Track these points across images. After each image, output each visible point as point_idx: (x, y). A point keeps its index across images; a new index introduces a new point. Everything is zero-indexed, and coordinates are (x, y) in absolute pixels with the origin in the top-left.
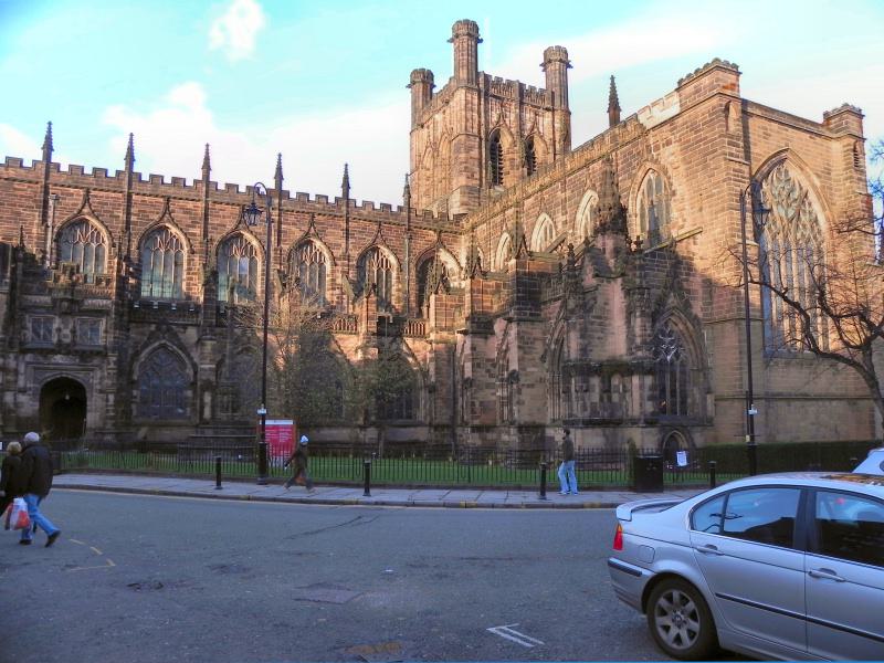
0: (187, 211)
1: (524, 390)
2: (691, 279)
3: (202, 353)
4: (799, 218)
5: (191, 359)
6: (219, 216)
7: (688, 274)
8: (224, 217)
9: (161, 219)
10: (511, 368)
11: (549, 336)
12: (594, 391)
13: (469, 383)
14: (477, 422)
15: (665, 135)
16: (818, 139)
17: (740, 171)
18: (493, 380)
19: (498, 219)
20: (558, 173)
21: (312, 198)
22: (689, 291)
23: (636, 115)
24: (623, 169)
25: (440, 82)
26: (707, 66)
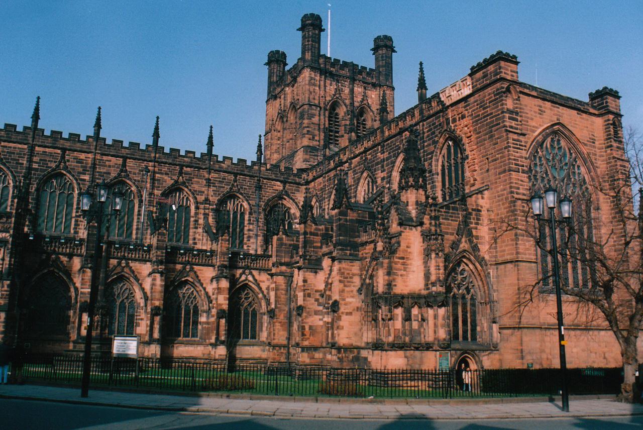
0: (80, 161)
1: (344, 317)
2: (479, 227)
4: (569, 179)
6: (106, 166)
7: (477, 224)
8: (110, 166)
9: (57, 166)
10: (334, 299)
11: (365, 273)
12: (397, 320)
13: (300, 309)
14: (306, 343)
15: (461, 110)
16: (584, 115)
17: (518, 140)
18: (321, 308)
19: (332, 174)
20: (379, 138)
21: (182, 153)
22: (477, 237)
23: (438, 93)
24: (428, 136)
25: (291, 61)
26: (492, 56)
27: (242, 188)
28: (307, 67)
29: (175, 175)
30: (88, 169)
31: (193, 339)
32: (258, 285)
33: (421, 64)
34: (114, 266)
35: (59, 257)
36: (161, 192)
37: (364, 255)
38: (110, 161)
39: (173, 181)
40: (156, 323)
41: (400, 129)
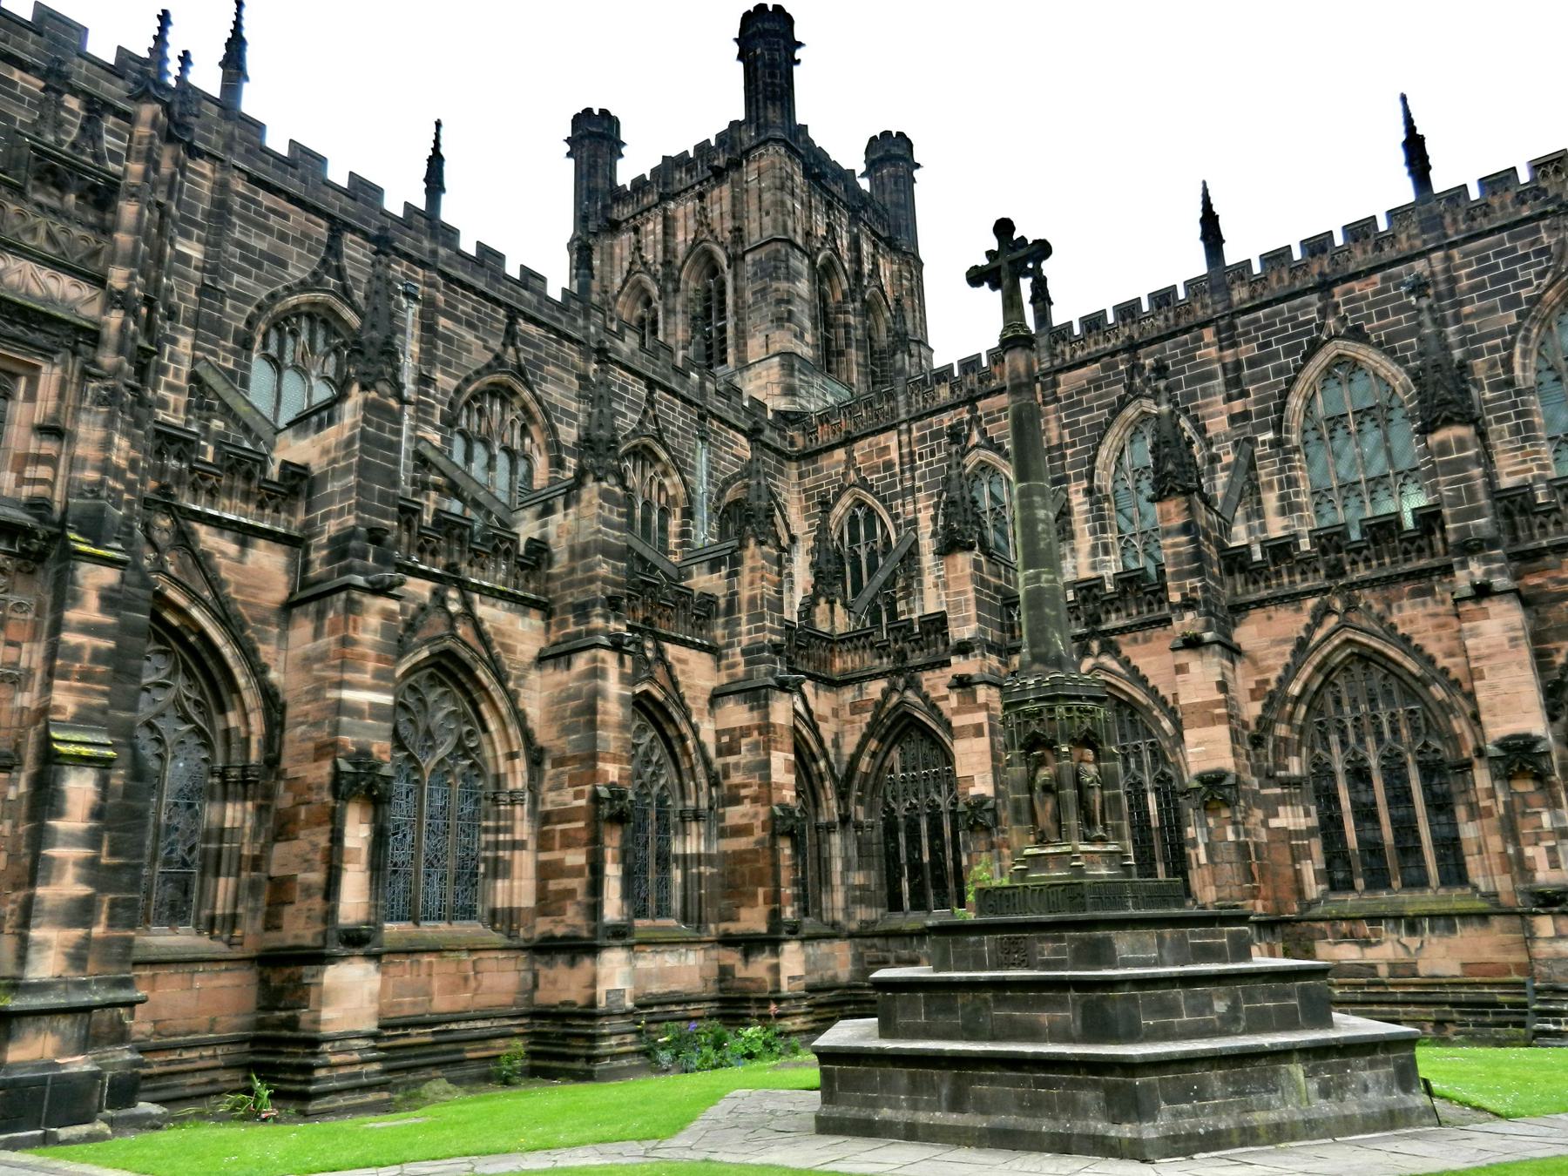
3: (346, 642)
5: (258, 670)
6: (268, 230)
8: (283, 237)
19: (947, 420)
24: (1472, 289)
27: (666, 429)
28: (777, 141)
29: (494, 335)
30: (199, 218)
31: (660, 922)
32: (815, 729)
33: (1404, 98)
34: (423, 608)
35: (194, 533)
36: (455, 383)
38: (285, 217)
39: (490, 356)
40: (609, 854)
41: (1399, 251)
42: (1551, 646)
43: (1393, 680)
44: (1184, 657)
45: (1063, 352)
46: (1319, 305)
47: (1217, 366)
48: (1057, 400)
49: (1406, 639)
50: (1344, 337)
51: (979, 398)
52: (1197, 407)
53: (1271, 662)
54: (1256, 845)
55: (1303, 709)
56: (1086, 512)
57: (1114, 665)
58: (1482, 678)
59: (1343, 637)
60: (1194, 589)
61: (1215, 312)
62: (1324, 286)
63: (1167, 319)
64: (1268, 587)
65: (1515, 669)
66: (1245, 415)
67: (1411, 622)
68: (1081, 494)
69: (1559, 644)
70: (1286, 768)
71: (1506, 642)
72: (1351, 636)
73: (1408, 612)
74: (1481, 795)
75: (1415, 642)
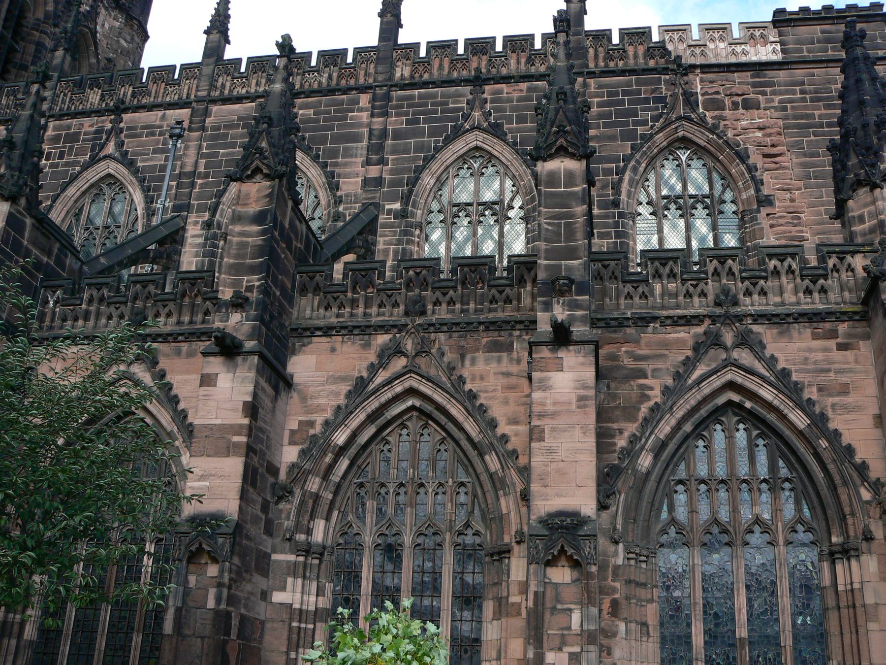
19: (88, 125)
24: (600, 116)
37: (627, 362)
42: (615, 426)
43: (451, 445)
44: (215, 365)
45: (223, 86)
46: (470, 97)
47: (366, 130)
48: (203, 128)
49: (472, 396)
50: (484, 131)
51: (126, 110)
52: (336, 165)
53: (322, 401)
54: (243, 619)
55: (344, 464)
56: (199, 245)
57: (146, 378)
58: (542, 439)
59: (407, 385)
60: (250, 289)
61: (375, 81)
62: (478, 81)
63: (330, 77)
64: (338, 316)
65: (577, 433)
66: (378, 182)
67: (482, 378)
68: (199, 227)
69: (622, 425)
70: (309, 532)
71: (574, 401)
72: (415, 385)
73: (481, 366)
74: (514, 589)
75: (481, 400)
